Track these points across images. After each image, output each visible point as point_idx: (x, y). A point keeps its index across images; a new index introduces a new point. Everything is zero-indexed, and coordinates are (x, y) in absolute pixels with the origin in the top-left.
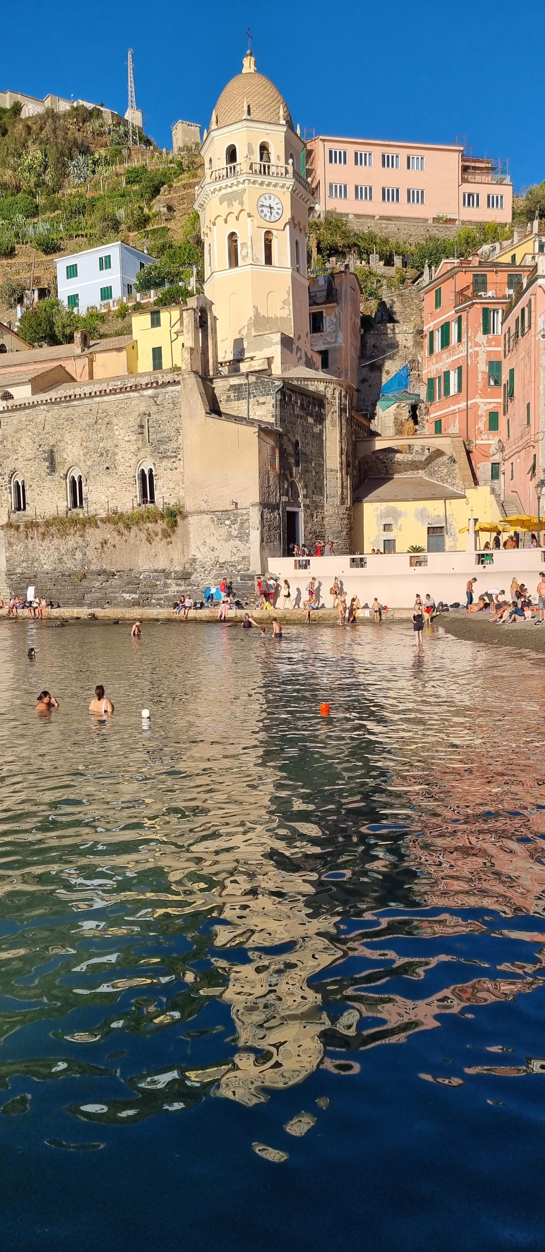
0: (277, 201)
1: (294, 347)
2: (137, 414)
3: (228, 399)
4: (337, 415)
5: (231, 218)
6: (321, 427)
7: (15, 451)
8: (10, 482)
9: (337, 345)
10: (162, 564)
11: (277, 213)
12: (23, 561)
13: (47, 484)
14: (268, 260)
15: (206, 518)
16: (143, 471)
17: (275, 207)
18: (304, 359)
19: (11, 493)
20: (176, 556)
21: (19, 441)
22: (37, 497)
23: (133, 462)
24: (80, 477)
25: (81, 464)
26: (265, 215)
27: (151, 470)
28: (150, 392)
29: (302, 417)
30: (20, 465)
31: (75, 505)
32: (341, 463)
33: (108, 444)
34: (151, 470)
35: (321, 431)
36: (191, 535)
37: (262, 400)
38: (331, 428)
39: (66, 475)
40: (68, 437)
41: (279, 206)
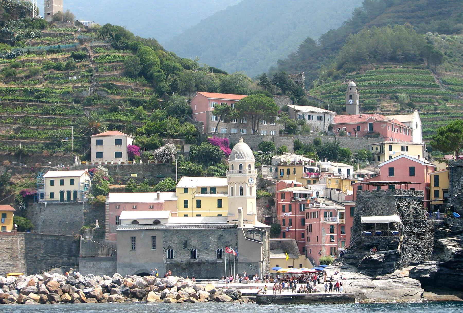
3: (247, 234)
8: (167, 250)
13: (183, 252)
16: (218, 250)
21: (172, 238)
22: (178, 255)
23: (216, 247)
25: (197, 247)
27: (221, 250)
30: (172, 245)
31: (192, 257)
33: (207, 242)
34: (221, 250)
37: (258, 235)
39: (190, 249)
40: (192, 239)
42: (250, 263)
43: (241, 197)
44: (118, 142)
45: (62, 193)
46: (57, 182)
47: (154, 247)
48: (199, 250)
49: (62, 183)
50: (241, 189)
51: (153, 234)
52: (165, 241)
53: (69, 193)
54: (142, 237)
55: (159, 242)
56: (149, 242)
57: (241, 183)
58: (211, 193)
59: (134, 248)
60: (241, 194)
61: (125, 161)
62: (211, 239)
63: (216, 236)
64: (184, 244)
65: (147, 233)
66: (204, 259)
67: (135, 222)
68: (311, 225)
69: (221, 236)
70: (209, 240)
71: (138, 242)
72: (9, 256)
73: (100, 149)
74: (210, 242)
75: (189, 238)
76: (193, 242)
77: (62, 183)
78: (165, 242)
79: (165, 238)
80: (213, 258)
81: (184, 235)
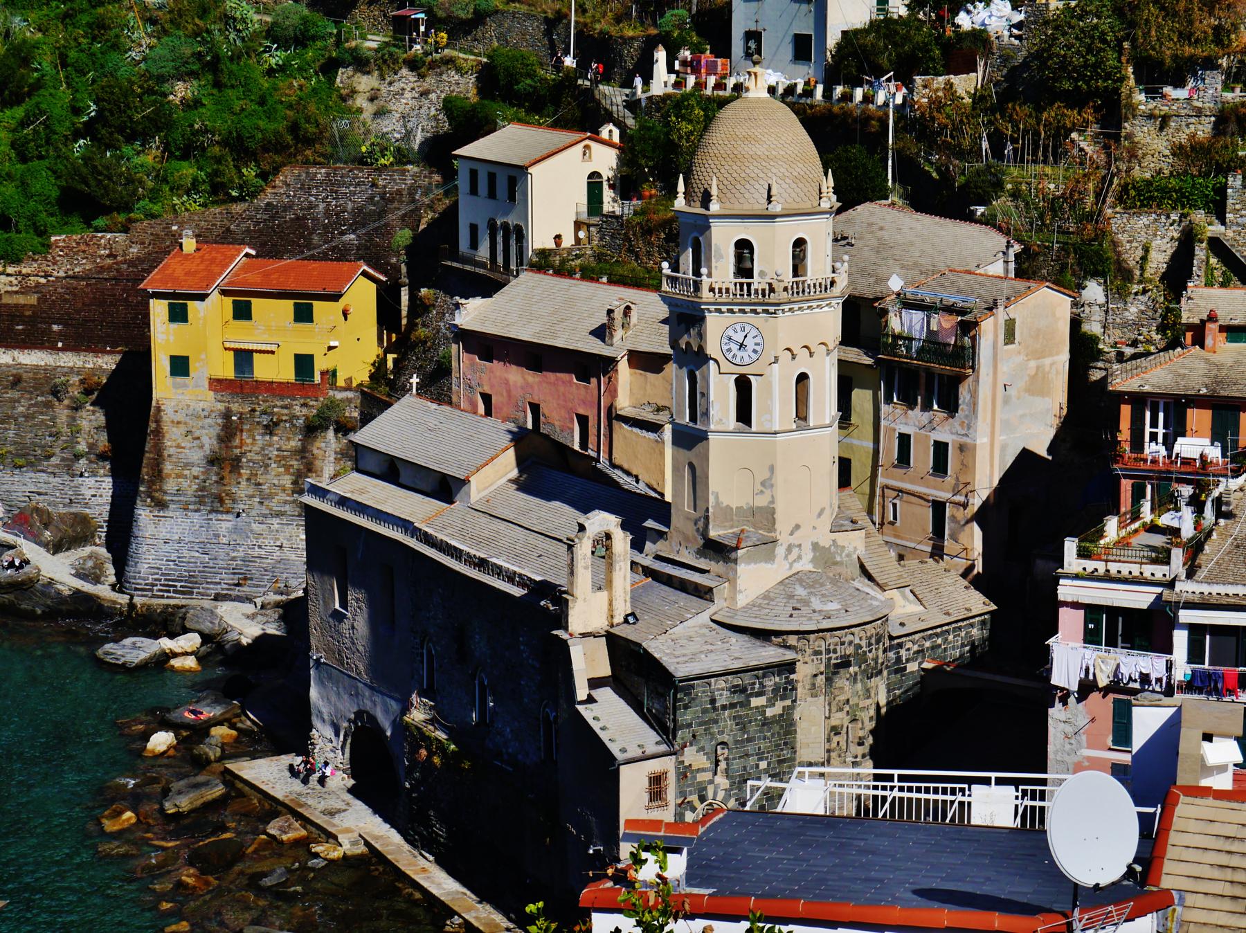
0: (754, 332)
1: (780, 551)
4: (821, 679)
6: (788, 702)
9: (968, 440)
11: (755, 351)
14: (744, 414)
17: (740, 354)
18: (808, 555)
19: (423, 662)
26: (734, 356)
29: (733, 706)
32: (829, 751)
35: (788, 711)
38: (809, 699)
41: (758, 340)
72: (289, 485)
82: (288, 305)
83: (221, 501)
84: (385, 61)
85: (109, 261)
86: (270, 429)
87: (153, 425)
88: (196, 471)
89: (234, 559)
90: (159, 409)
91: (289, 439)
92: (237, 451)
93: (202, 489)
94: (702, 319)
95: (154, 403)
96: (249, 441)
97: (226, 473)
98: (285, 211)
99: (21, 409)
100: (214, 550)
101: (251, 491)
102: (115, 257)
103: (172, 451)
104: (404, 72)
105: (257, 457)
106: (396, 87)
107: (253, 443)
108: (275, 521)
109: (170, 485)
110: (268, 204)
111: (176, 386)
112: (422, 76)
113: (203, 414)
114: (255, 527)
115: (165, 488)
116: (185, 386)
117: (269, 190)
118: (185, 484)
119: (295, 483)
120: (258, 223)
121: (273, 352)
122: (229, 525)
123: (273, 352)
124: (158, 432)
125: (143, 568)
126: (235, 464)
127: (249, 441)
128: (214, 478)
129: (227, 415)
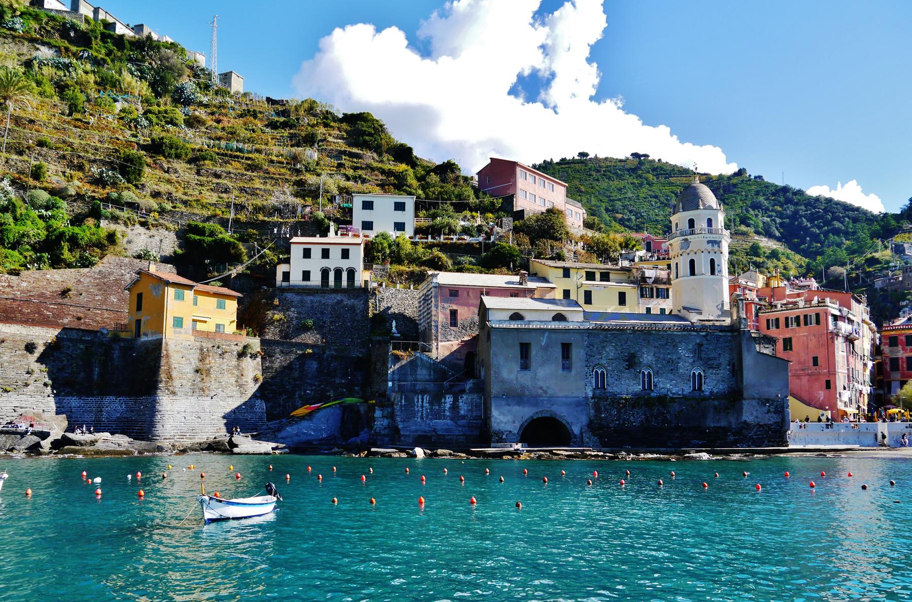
2: (694, 343)
5: (712, 253)
7: (600, 354)
8: (593, 371)
10: (723, 423)
12: (616, 420)
15: (754, 403)
16: (694, 373)
20: (733, 420)
21: (604, 347)
22: (616, 382)
24: (649, 373)
25: (654, 366)
27: (700, 373)
28: (704, 333)
30: (604, 362)
34: (700, 373)
36: (744, 410)
37: (767, 346)
40: (644, 350)
42: (768, 400)
43: (713, 277)
44: (400, 207)
45: (325, 273)
46: (316, 252)
47: (567, 367)
48: (657, 373)
49: (326, 254)
50: (712, 261)
51: (566, 339)
52: (589, 353)
53: (338, 272)
54: (543, 344)
55: (578, 354)
56: (558, 352)
57: (712, 253)
58: (601, 280)
59: (525, 366)
60: (713, 272)
61: (227, 323)
62: (682, 351)
63: (690, 347)
64: (627, 361)
65: (553, 336)
66: (668, 390)
67: (516, 316)
68: (790, 339)
69: (700, 345)
70: (678, 353)
71: (534, 352)
72: (233, 380)
73: (367, 215)
74: (679, 358)
75: (637, 349)
76: (647, 357)
77: (326, 254)
78: (591, 356)
79: (589, 347)
80: (687, 389)
81: (629, 343)
82: (214, 300)
83: (203, 390)
84: (129, 220)
85: (8, 290)
86: (222, 355)
87: (164, 352)
88: (189, 376)
89: (213, 419)
90: (167, 344)
91: (231, 361)
92: (208, 366)
93: (194, 385)
94: (721, 241)
95: (164, 341)
96: (213, 361)
97: (204, 376)
98: (109, 275)
99: (5, 358)
100: (202, 415)
101: (217, 385)
102: (12, 287)
103: (176, 366)
104: (137, 226)
105: (217, 369)
106: (135, 232)
107: (214, 361)
108: (230, 399)
109: (177, 383)
110: (100, 271)
111: (175, 332)
112: (148, 229)
113: (189, 347)
114: (221, 403)
115: (174, 384)
116: (180, 333)
117: (101, 264)
118: (184, 382)
119: (237, 381)
120: (96, 279)
121: (205, 322)
122: (208, 402)
123: (205, 322)
124: (167, 356)
125: (168, 426)
126: (208, 371)
127: (213, 361)
128: (199, 379)
129: (201, 350)
